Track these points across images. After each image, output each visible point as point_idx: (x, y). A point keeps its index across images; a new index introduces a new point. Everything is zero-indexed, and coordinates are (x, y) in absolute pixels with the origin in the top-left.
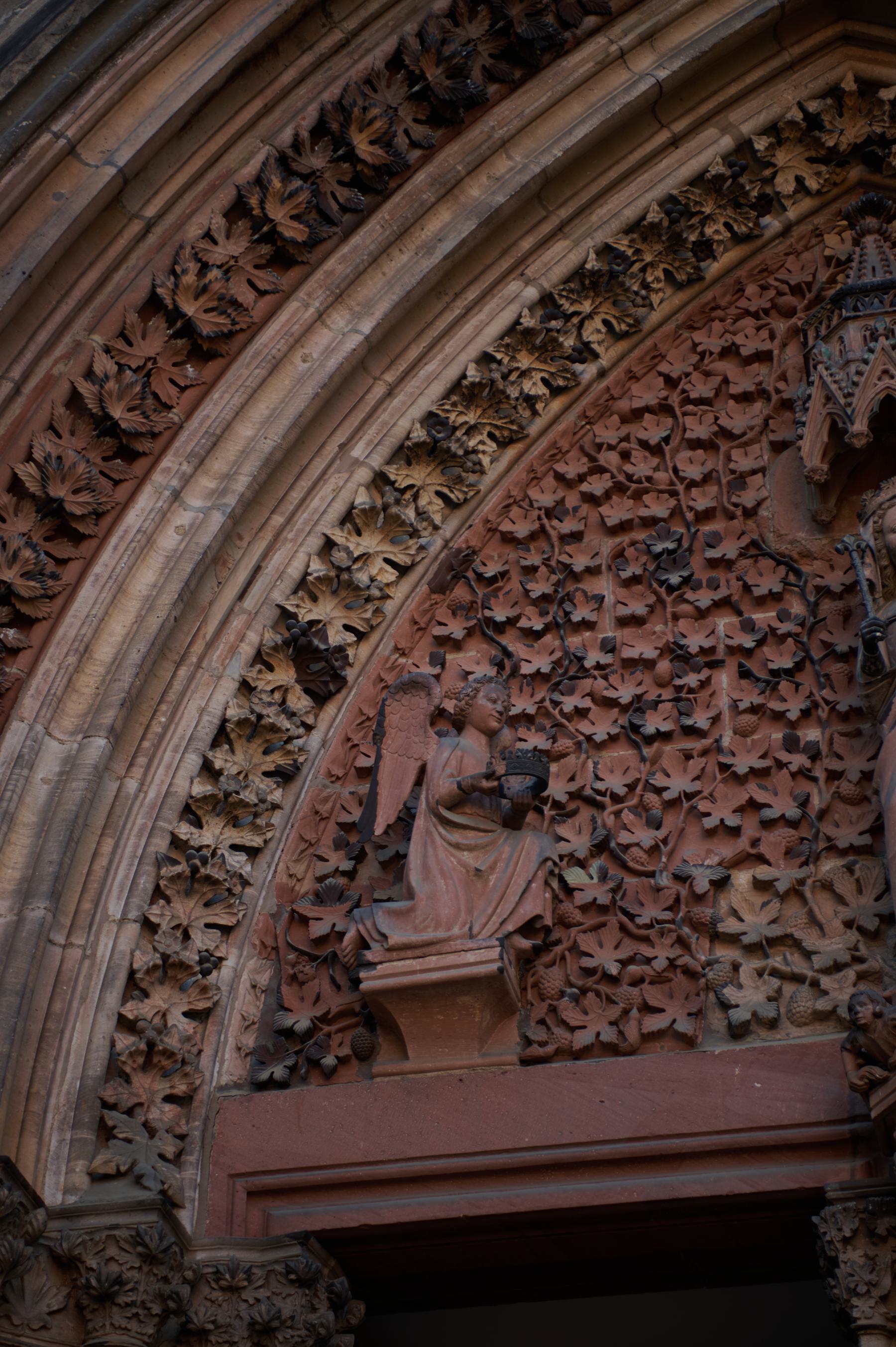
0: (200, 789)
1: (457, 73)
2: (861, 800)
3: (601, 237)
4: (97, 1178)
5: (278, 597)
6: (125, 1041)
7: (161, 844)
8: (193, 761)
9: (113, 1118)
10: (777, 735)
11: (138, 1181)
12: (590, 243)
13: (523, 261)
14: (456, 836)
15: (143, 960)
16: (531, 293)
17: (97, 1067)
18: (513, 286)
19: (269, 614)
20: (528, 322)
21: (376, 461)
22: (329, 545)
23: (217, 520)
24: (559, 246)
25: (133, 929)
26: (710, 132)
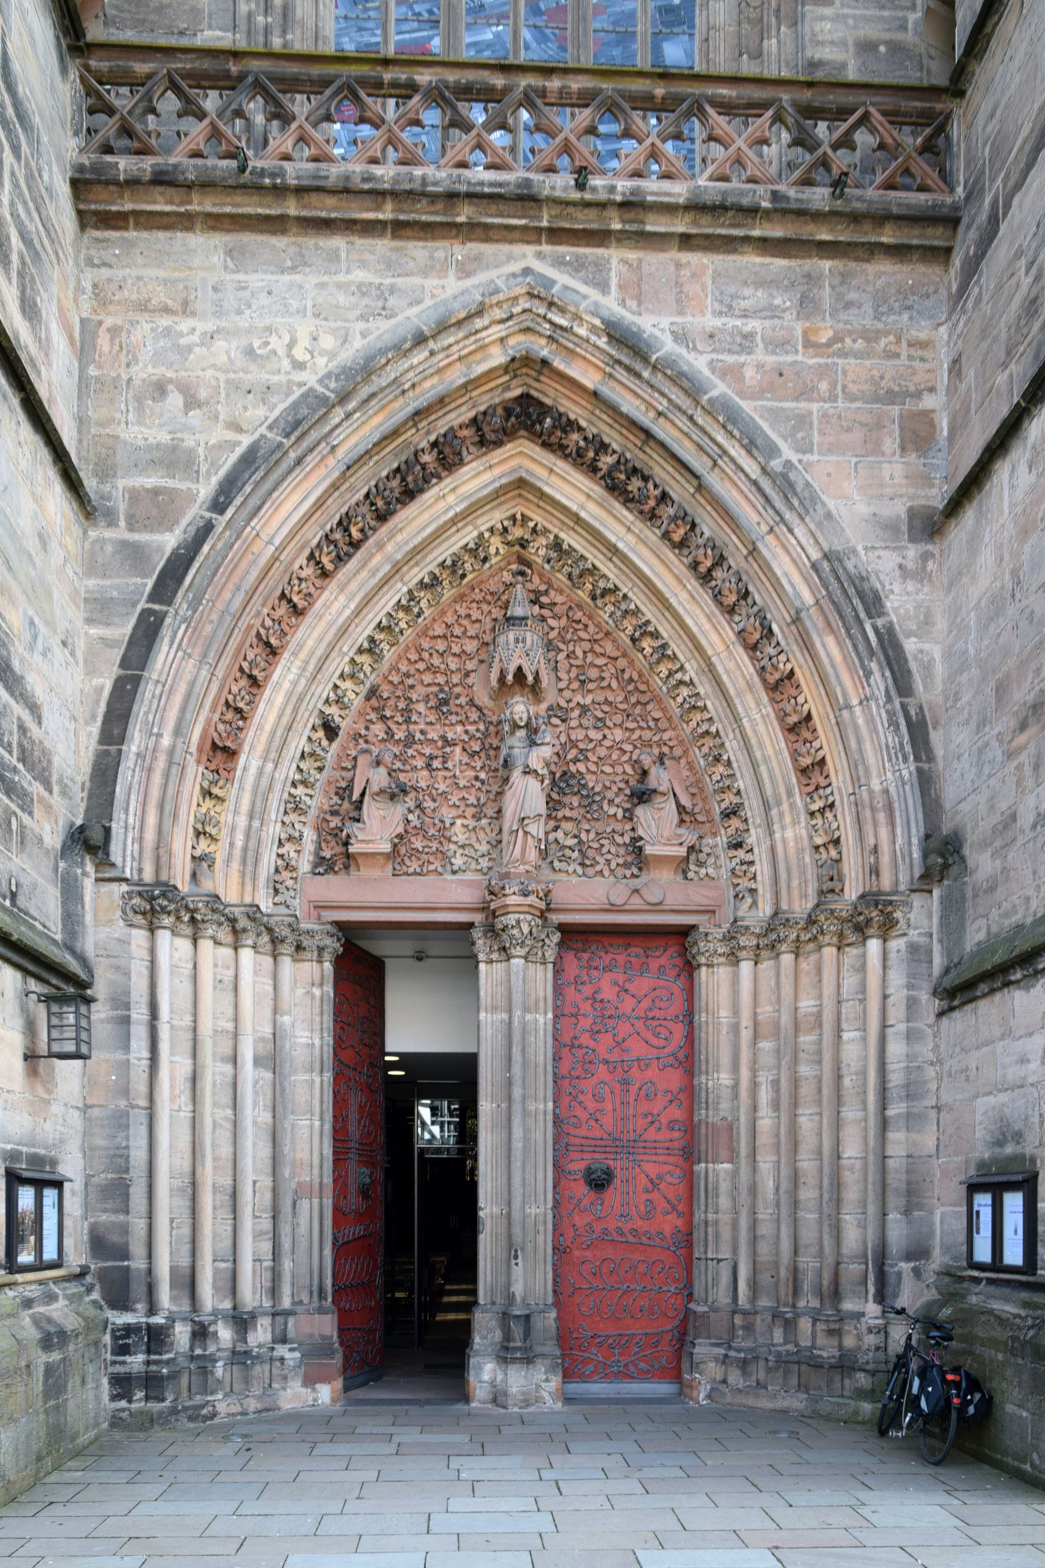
0: (298, 777)
1: (388, 504)
2: (495, 801)
3: (430, 568)
4: (275, 904)
5: (320, 705)
6: (280, 862)
7: (286, 796)
8: (294, 766)
9: (278, 886)
10: (473, 774)
11: (288, 907)
12: (426, 570)
13: (403, 576)
14: (378, 805)
15: (284, 836)
16: (405, 589)
17: (272, 870)
18: (399, 585)
19: (316, 712)
20: (404, 602)
21: (351, 654)
22: (336, 687)
23: (303, 681)
24: (416, 570)
25: (279, 824)
26: (470, 528)
